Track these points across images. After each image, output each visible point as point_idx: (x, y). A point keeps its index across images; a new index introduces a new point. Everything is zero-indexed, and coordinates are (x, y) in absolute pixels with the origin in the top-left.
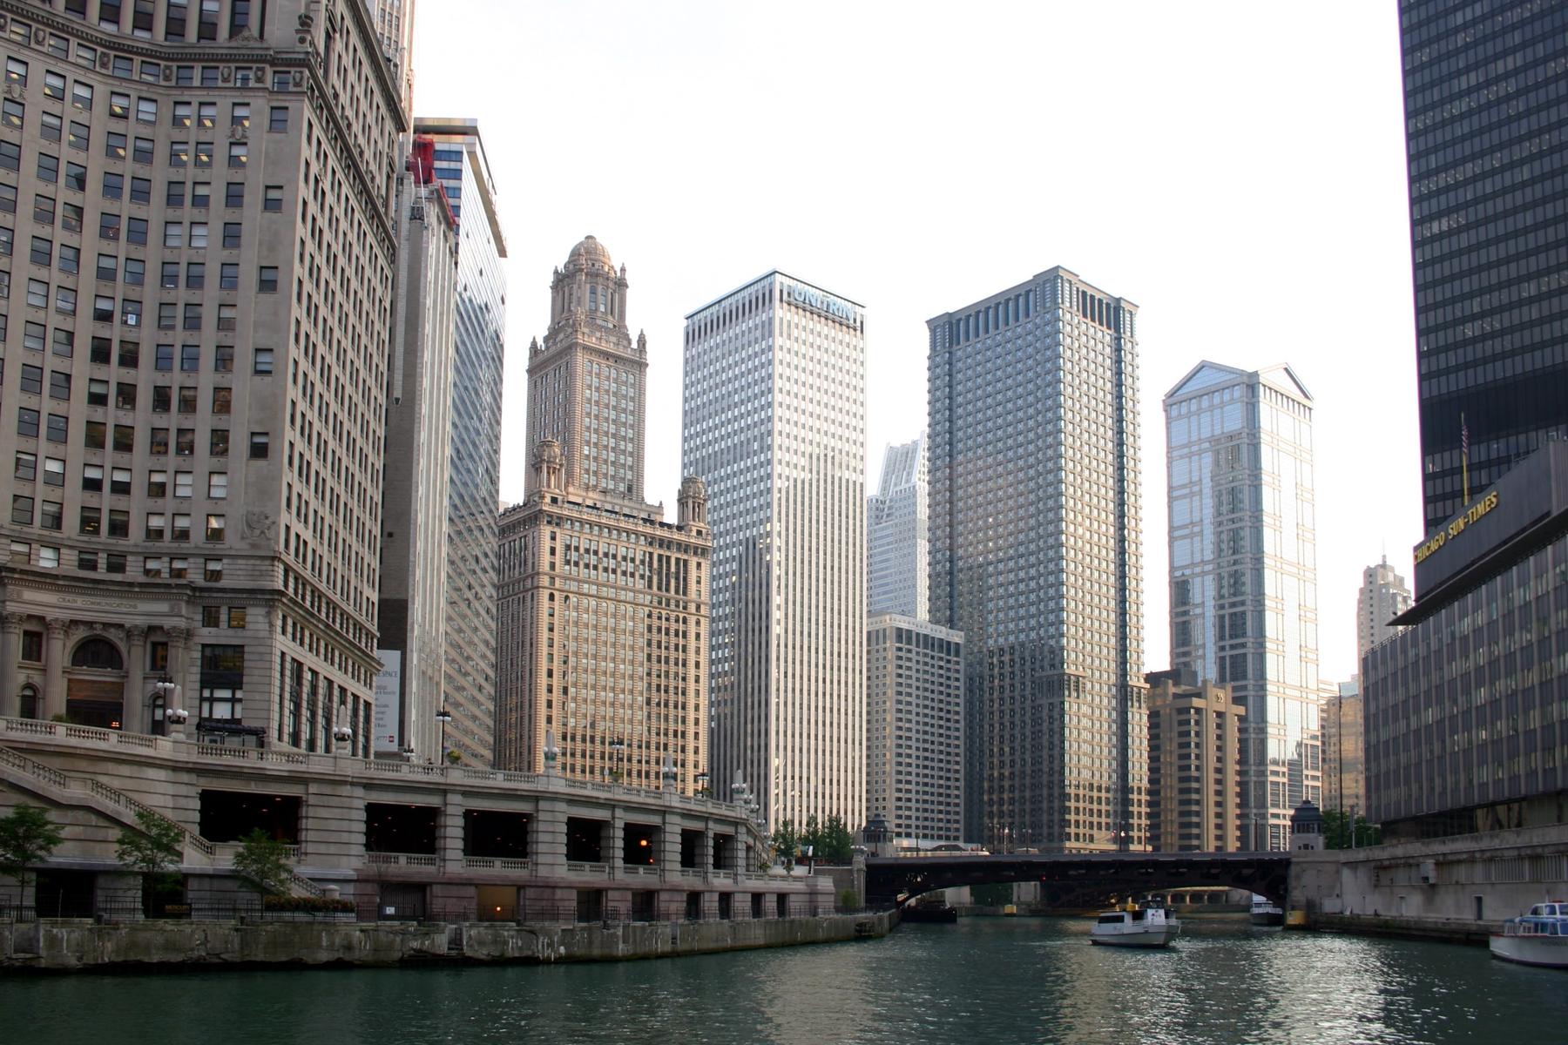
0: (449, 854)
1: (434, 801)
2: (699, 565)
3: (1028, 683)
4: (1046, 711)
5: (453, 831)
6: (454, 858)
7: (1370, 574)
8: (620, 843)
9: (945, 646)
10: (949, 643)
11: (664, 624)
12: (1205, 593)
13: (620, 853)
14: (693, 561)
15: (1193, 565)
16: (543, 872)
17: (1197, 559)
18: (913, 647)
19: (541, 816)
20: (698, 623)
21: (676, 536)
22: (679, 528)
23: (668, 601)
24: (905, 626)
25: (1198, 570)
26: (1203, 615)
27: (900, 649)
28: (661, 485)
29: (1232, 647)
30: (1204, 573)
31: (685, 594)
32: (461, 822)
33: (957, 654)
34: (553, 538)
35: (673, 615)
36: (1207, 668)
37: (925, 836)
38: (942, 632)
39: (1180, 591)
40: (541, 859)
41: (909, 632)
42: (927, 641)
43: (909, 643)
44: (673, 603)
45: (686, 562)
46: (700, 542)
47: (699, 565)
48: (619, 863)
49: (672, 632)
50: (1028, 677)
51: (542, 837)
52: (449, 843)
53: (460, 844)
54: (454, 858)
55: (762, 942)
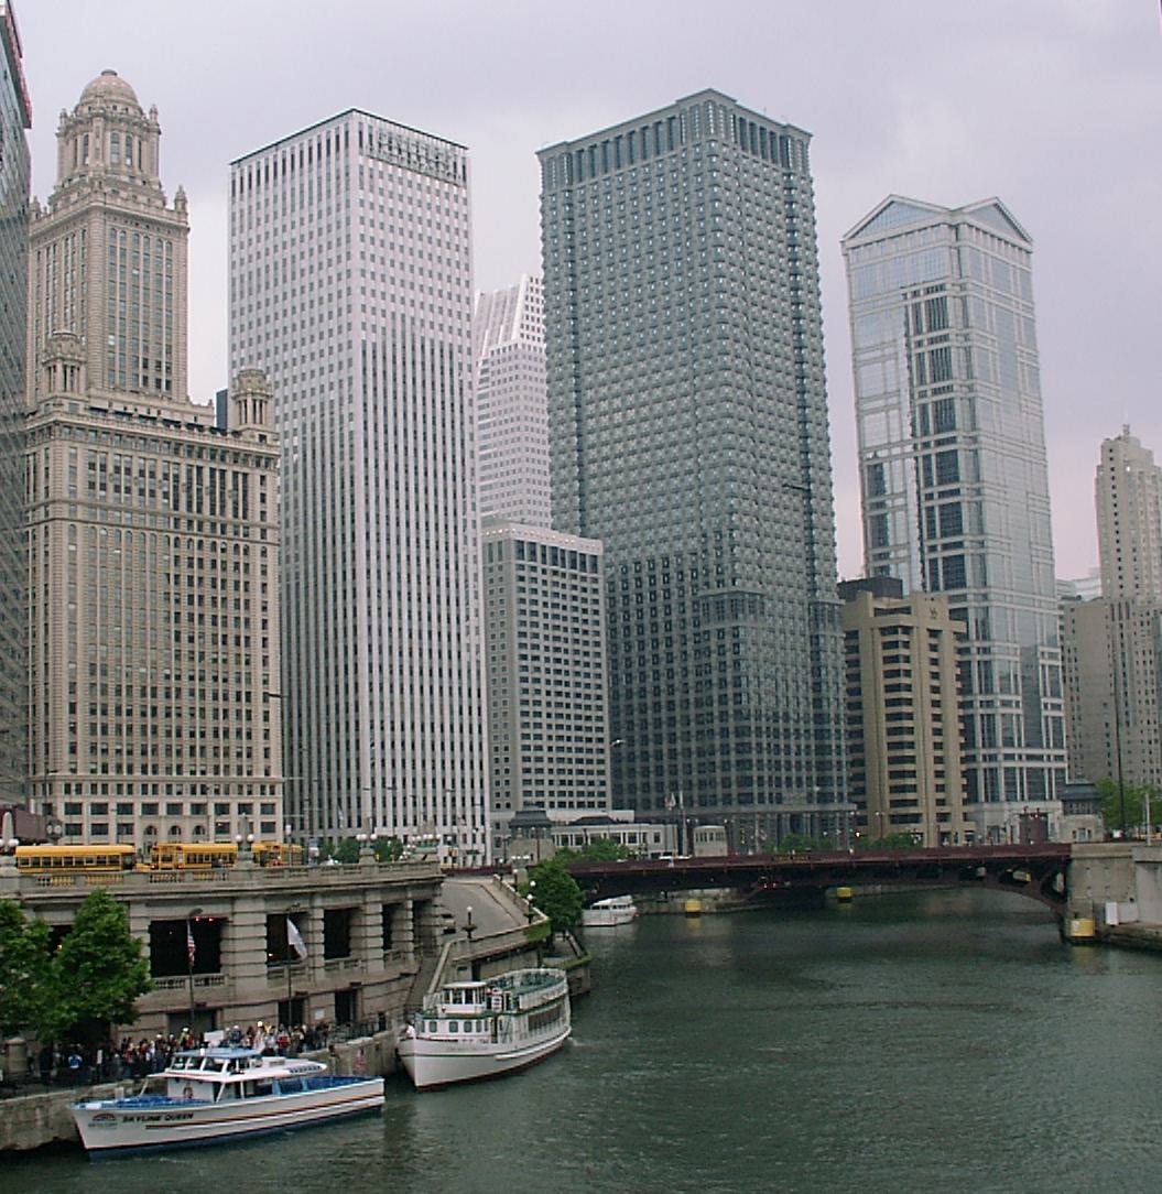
2: (263, 478)
3: (688, 604)
4: (713, 643)
7: (1109, 450)
9: (577, 560)
10: (583, 555)
11: (219, 557)
12: (903, 478)
15: (889, 445)
17: (895, 439)
18: (540, 566)
20: (264, 553)
21: (230, 443)
22: (236, 434)
23: (223, 527)
25: (896, 451)
26: (905, 507)
27: (522, 567)
28: (206, 374)
29: (946, 547)
30: (903, 456)
33: (595, 567)
35: (231, 545)
36: (909, 573)
38: (569, 542)
39: (874, 478)
42: (556, 555)
44: (230, 529)
46: (264, 450)
47: (263, 478)
49: (230, 566)
50: (689, 595)
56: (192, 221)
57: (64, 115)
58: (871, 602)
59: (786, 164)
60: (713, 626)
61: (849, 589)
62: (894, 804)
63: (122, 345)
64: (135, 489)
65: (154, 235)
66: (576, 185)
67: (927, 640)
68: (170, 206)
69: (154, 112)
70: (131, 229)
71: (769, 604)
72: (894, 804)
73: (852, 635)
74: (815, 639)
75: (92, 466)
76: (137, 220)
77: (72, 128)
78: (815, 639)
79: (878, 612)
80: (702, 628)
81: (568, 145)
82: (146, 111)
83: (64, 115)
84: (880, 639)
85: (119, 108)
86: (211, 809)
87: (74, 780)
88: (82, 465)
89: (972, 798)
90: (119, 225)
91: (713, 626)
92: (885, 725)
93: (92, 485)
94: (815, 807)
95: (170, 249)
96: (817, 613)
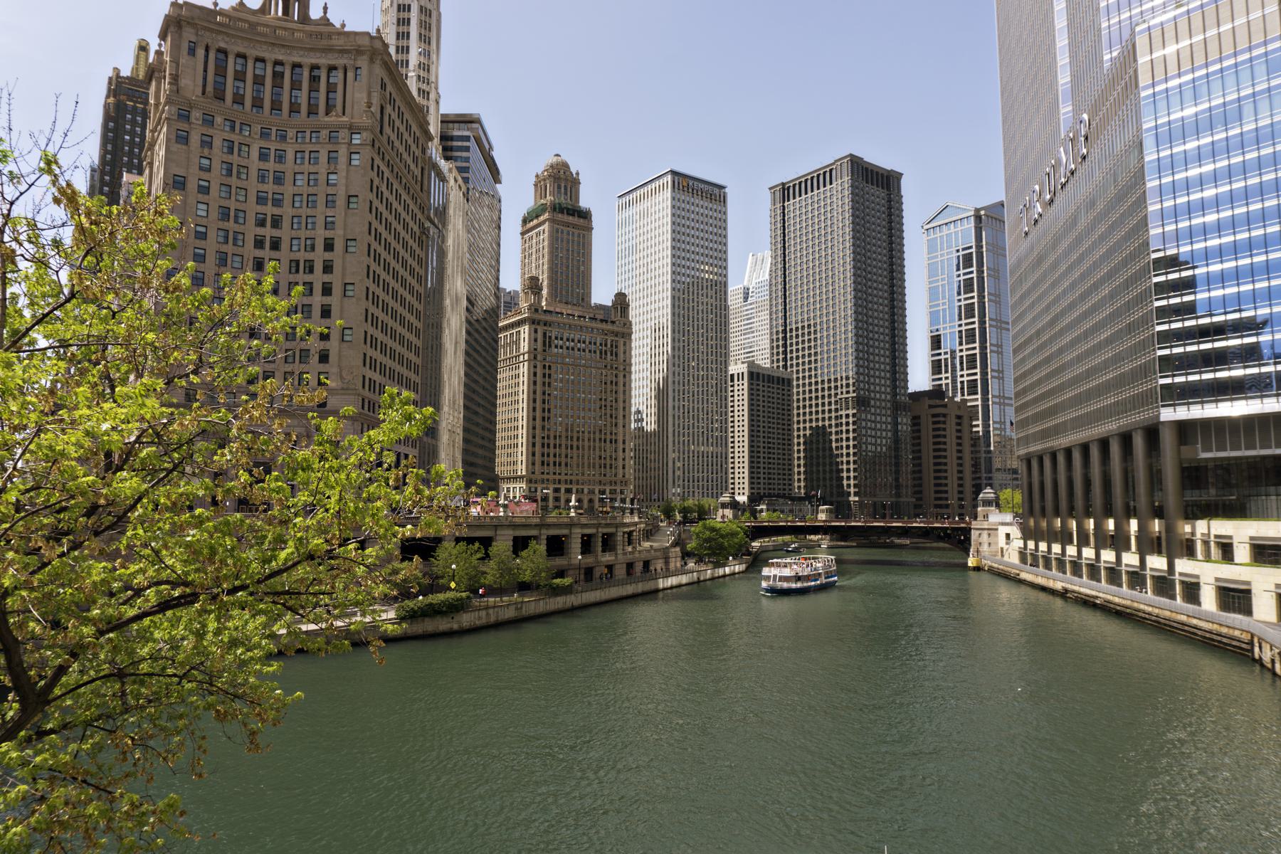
14: (622, 341)
24: (755, 370)
34: (536, 331)
41: (758, 374)
46: (625, 330)
57: (537, 176)
58: (928, 402)
59: (888, 189)
60: (843, 413)
61: (918, 396)
62: (936, 499)
67: (954, 421)
69: (578, 174)
70: (566, 229)
71: (872, 402)
72: (936, 499)
78: (895, 418)
79: (931, 407)
81: (783, 184)
84: (931, 420)
91: (843, 413)
96: (897, 407)
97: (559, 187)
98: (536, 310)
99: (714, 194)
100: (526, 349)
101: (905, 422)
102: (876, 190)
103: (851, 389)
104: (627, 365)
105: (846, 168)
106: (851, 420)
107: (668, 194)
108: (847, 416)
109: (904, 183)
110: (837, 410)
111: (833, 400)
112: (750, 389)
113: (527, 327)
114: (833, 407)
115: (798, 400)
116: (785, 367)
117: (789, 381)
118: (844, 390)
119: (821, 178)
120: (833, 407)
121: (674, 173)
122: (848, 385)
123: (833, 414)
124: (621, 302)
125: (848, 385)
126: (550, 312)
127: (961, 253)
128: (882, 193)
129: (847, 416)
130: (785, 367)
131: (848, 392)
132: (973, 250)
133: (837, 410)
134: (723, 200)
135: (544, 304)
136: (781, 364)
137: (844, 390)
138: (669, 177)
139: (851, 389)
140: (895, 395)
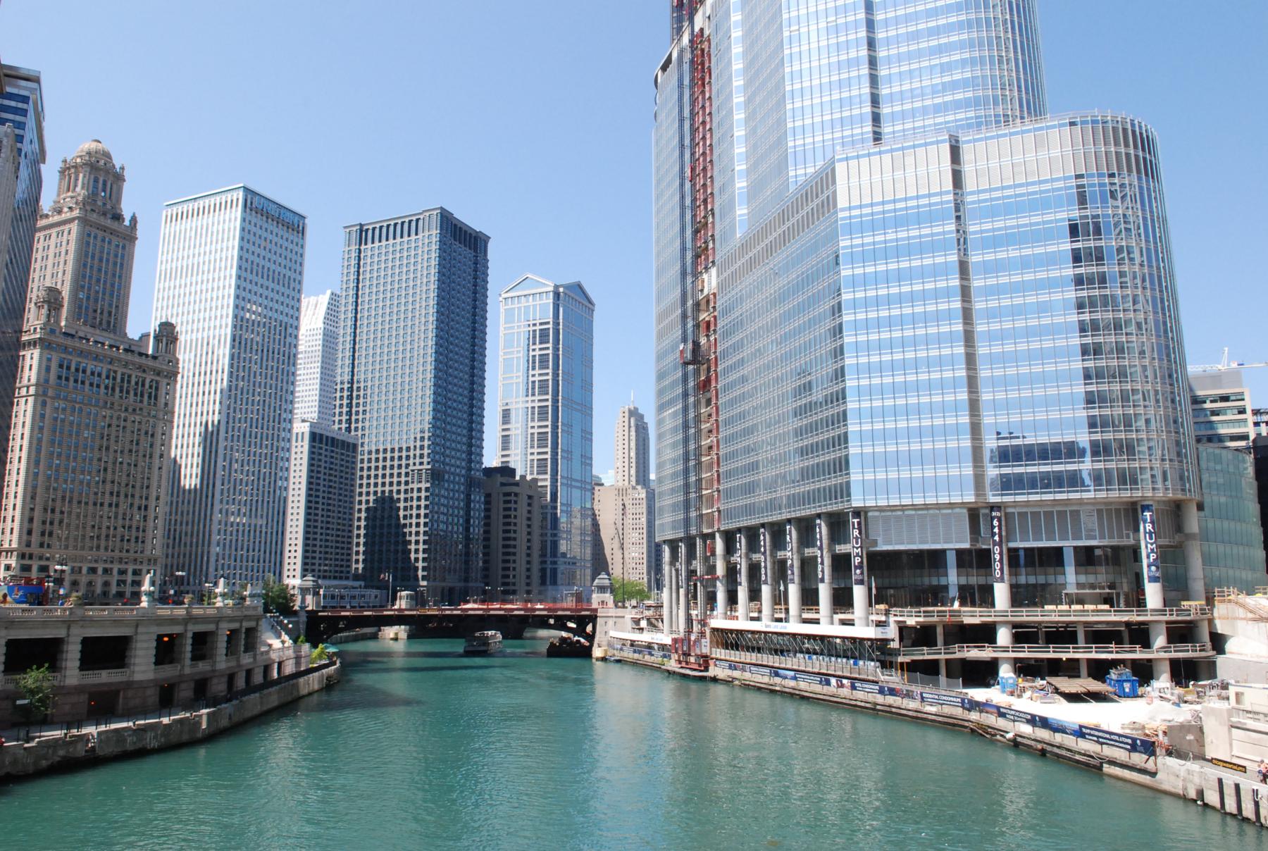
0: (68, 673)
1: (60, 633)
5: (73, 653)
6: (72, 673)
8: (189, 648)
13: (189, 655)
16: (138, 677)
19: (140, 637)
21: (150, 363)
22: (154, 358)
24: (318, 431)
31: (155, 404)
32: (79, 647)
34: (49, 360)
37: (325, 577)
40: (137, 669)
41: (321, 435)
43: (321, 442)
45: (157, 382)
48: (188, 662)
51: (139, 653)
52: (69, 664)
53: (78, 664)
54: (72, 673)
55: (276, 703)
56: (139, 233)
57: (65, 161)
58: (500, 479)
59: (475, 251)
60: (415, 486)
61: (490, 472)
63: (88, 298)
64: (87, 383)
65: (115, 241)
66: (363, 247)
67: (525, 500)
68: (127, 223)
69: (123, 168)
70: (100, 234)
73: (488, 496)
74: (468, 496)
75: (61, 366)
76: (104, 229)
77: (67, 170)
78: (468, 496)
79: (503, 484)
80: (411, 486)
81: (361, 225)
82: (118, 167)
83: (65, 161)
84: (502, 498)
85: (102, 162)
86: (115, 572)
87: (27, 551)
88: (54, 365)
89: (543, 583)
90: (94, 231)
92: (501, 543)
93: (60, 377)
94: (462, 584)
95: (124, 248)
96: (471, 483)
97: (96, 180)
98: (52, 331)
99: (293, 224)
100: (33, 381)
101: (478, 498)
102: (463, 250)
103: (426, 460)
104: (169, 410)
105: (435, 221)
106: (423, 494)
107: (238, 213)
108: (419, 490)
109: (490, 245)
110: (407, 483)
111: (403, 471)
112: (311, 453)
113: (36, 352)
114: (403, 479)
115: (362, 469)
116: (349, 429)
117: (355, 446)
118: (418, 461)
119: (407, 227)
120: (403, 479)
121: (246, 189)
122: (422, 456)
123: (403, 487)
124: (167, 334)
125: (422, 456)
126: (73, 336)
127: (538, 328)
128: (469, 253)
129: (419, 490)
130: (349, 429)
131: (421, 464)
132: (550, 326)
133: (407, 483)
134: (301, 231)
135: (63, 324)
136: (344, 426)
137: (418, 461)
138: (241, 194)
139: (426, 460)
140: (470, 469)
